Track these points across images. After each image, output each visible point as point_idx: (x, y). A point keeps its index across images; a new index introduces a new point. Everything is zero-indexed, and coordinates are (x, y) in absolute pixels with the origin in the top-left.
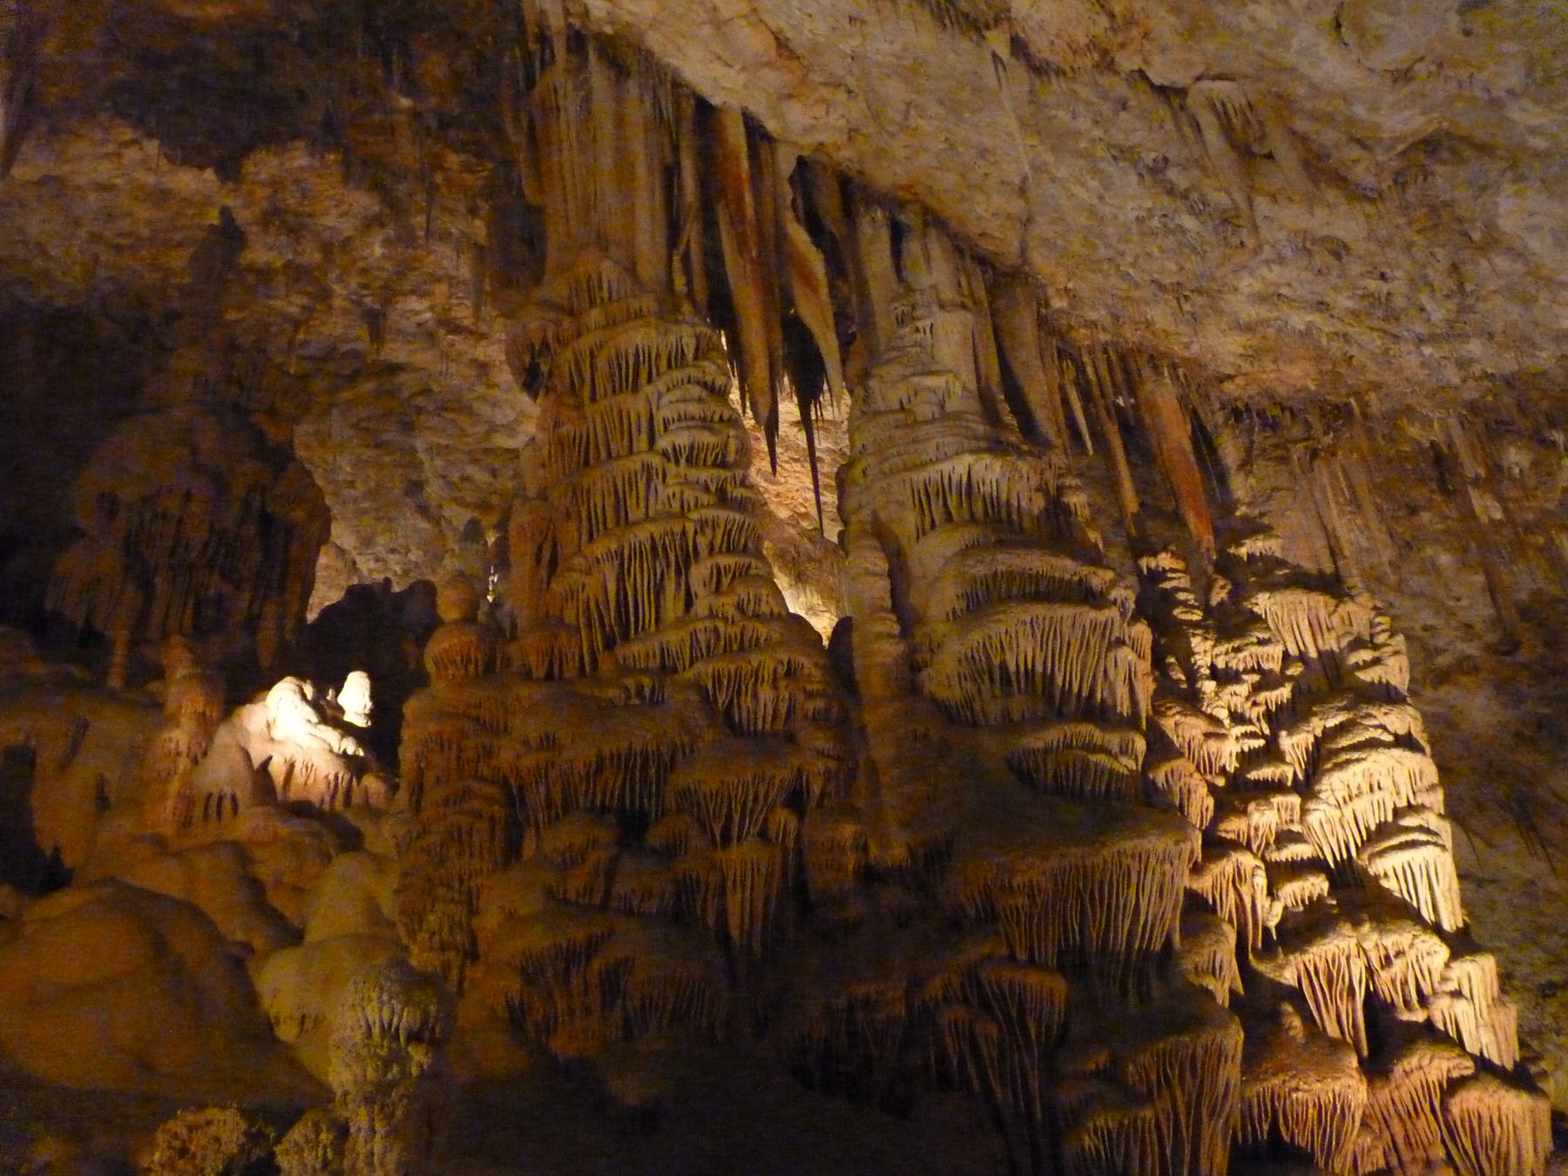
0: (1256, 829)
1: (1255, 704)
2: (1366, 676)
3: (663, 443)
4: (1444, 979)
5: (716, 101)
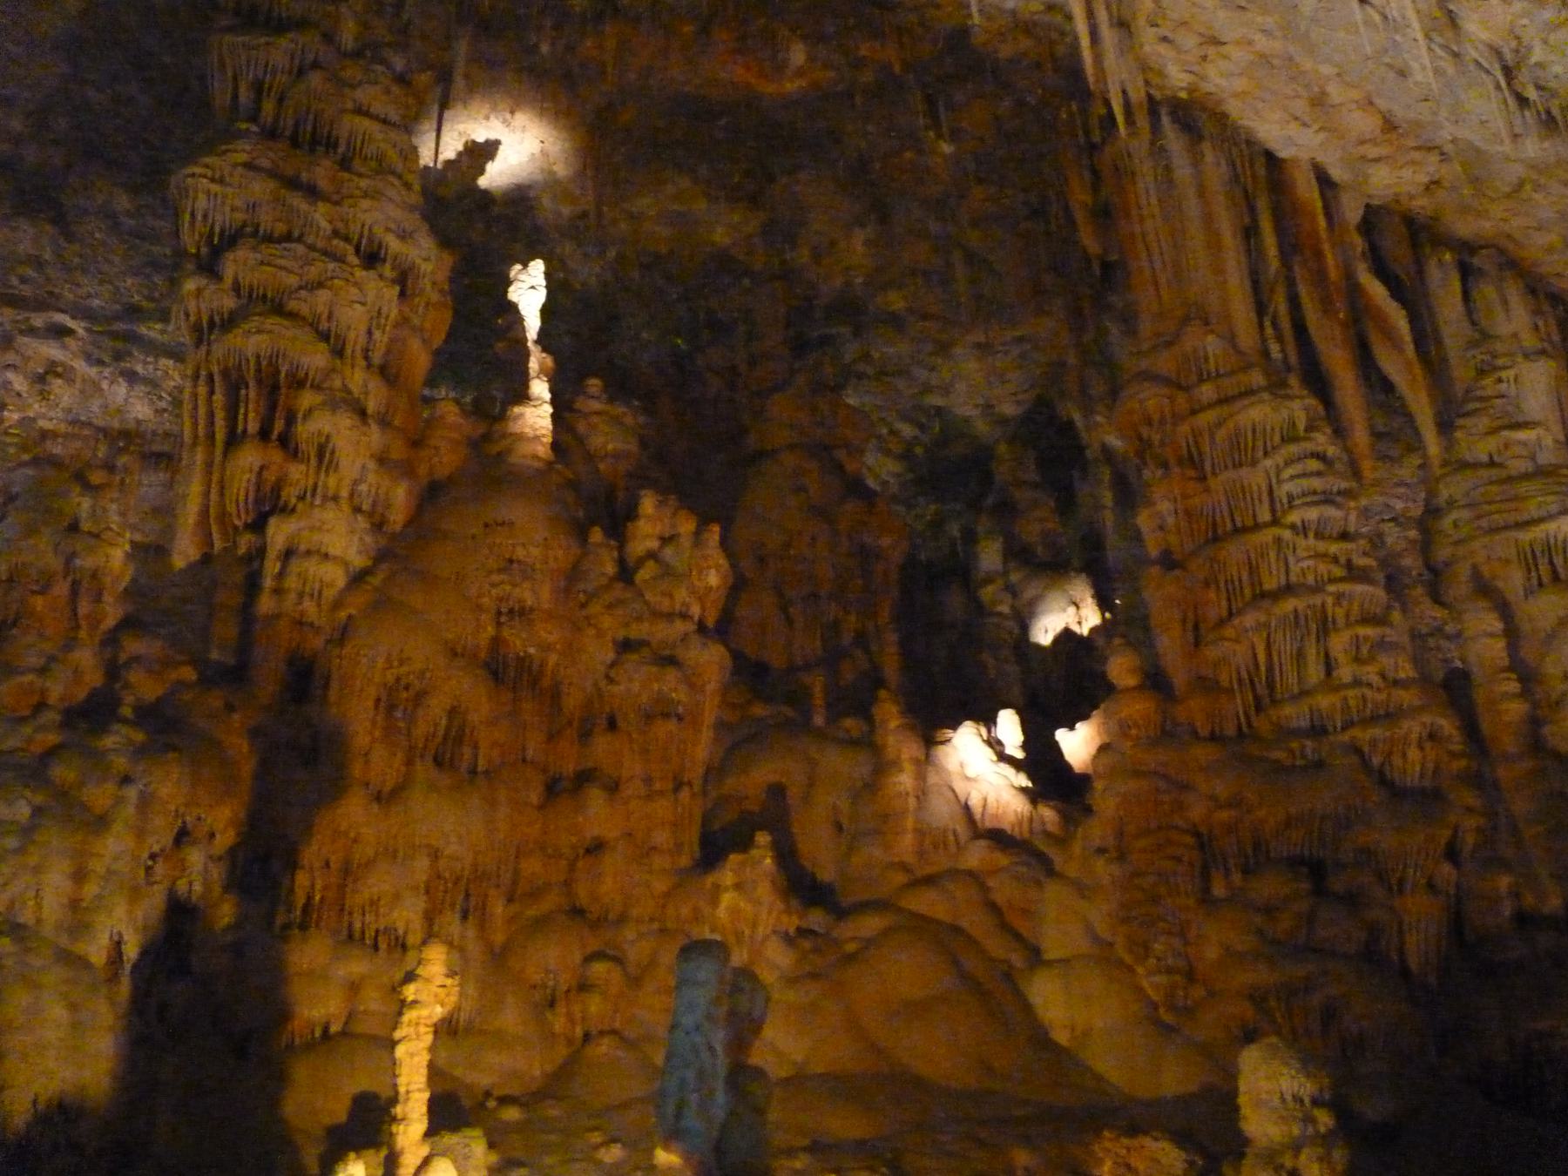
3: (1294, 517)
5: (1283, 154)
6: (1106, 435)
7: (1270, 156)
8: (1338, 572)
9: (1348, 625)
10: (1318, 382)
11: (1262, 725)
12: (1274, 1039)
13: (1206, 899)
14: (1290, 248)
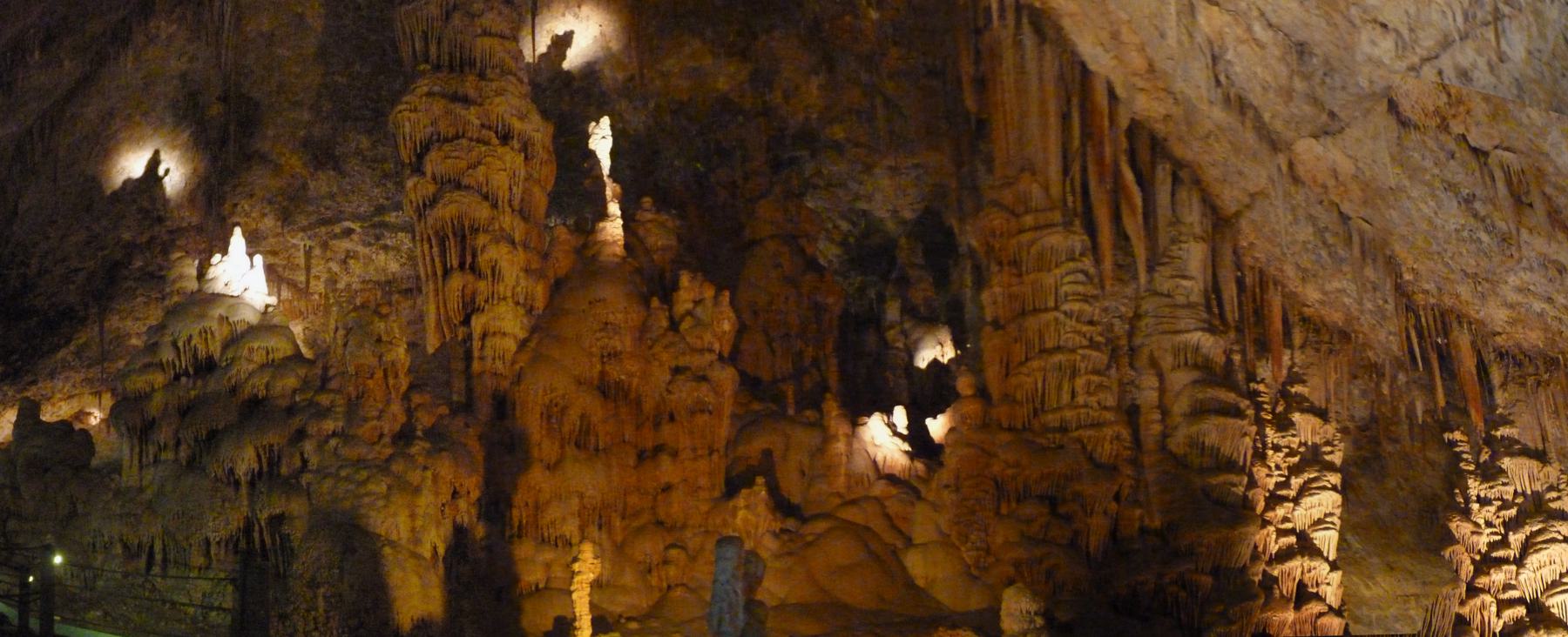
2: (1328, 458)
6: (970, 238)
7: (1083, 65)
8: (1085, 343)
9: (1086, 373)
10: (1091, 230)
11: (1036, 425)
12: (1020, 585)
13: (998, 513)
14: (1086, 135)
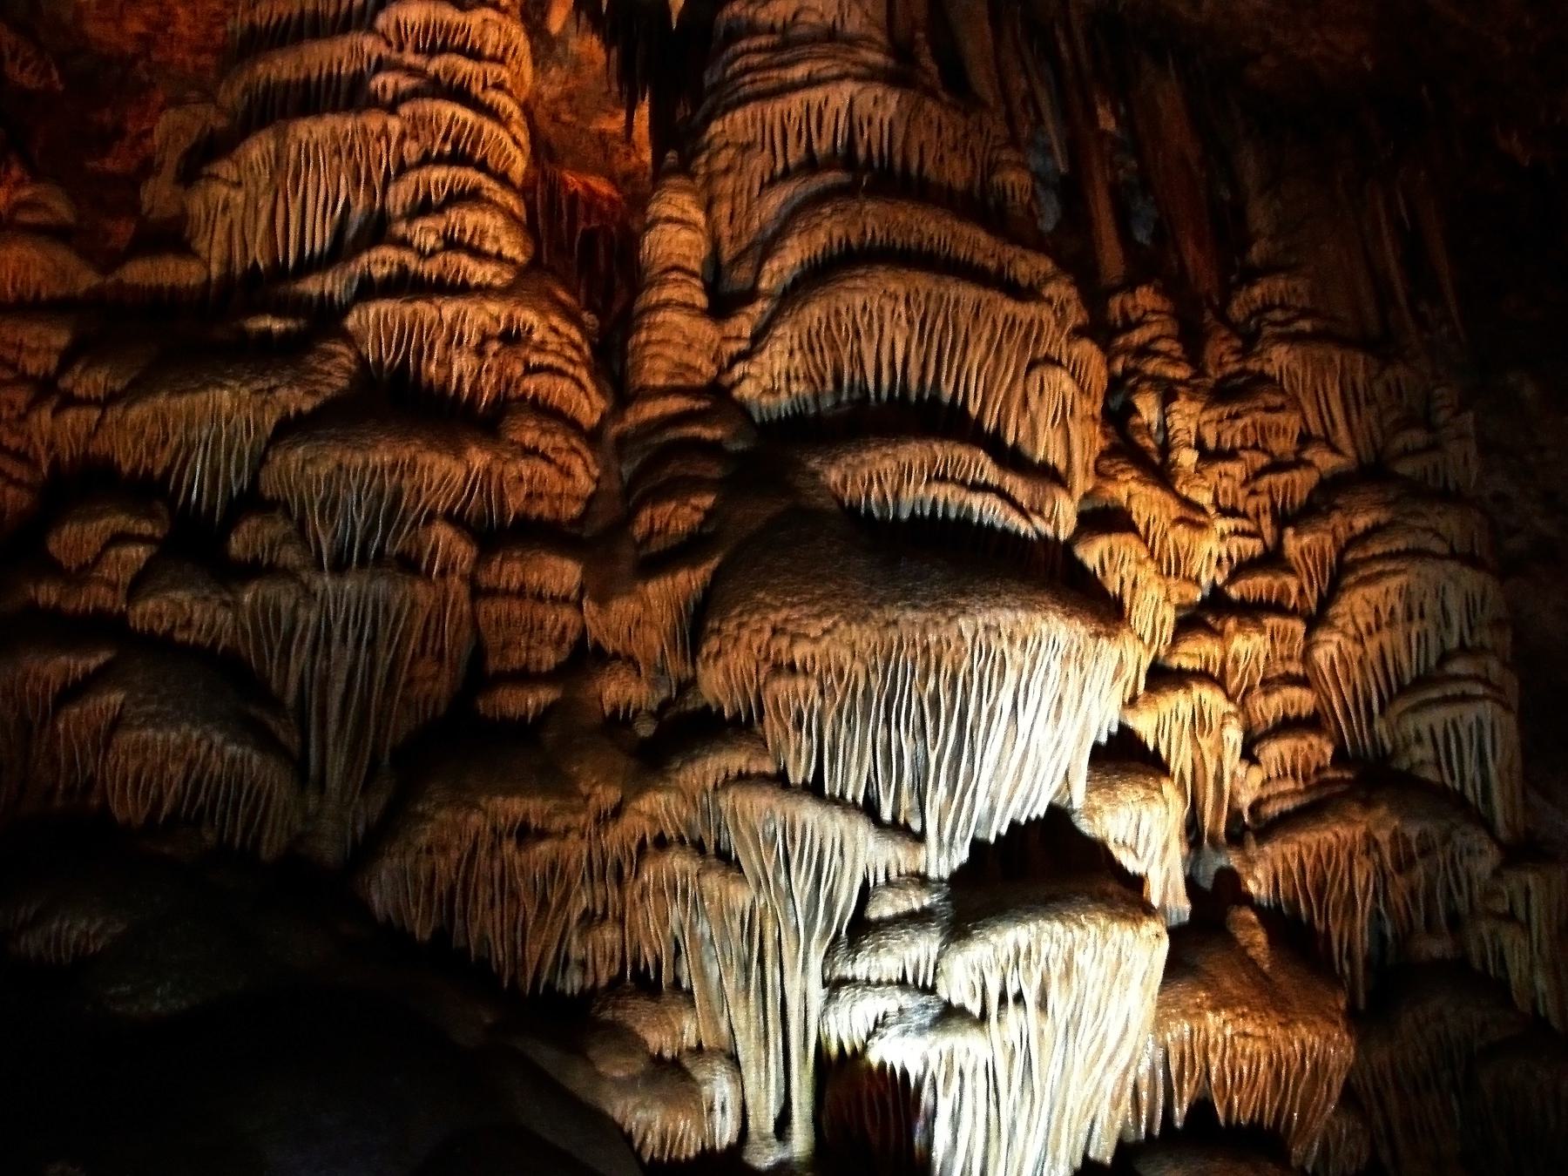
0: (1236, 661)
1: (1253, 493)
4: (1489, 894)
